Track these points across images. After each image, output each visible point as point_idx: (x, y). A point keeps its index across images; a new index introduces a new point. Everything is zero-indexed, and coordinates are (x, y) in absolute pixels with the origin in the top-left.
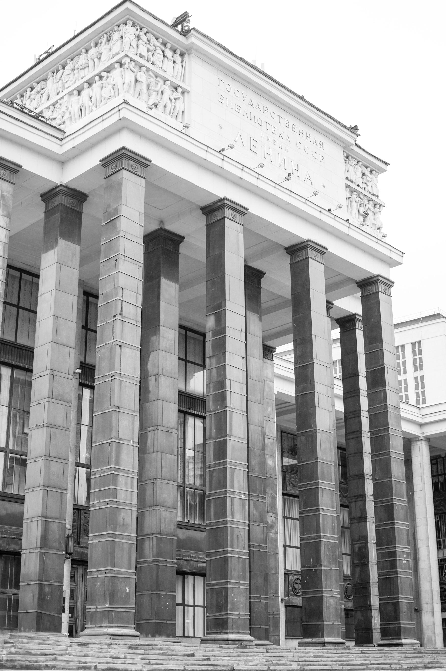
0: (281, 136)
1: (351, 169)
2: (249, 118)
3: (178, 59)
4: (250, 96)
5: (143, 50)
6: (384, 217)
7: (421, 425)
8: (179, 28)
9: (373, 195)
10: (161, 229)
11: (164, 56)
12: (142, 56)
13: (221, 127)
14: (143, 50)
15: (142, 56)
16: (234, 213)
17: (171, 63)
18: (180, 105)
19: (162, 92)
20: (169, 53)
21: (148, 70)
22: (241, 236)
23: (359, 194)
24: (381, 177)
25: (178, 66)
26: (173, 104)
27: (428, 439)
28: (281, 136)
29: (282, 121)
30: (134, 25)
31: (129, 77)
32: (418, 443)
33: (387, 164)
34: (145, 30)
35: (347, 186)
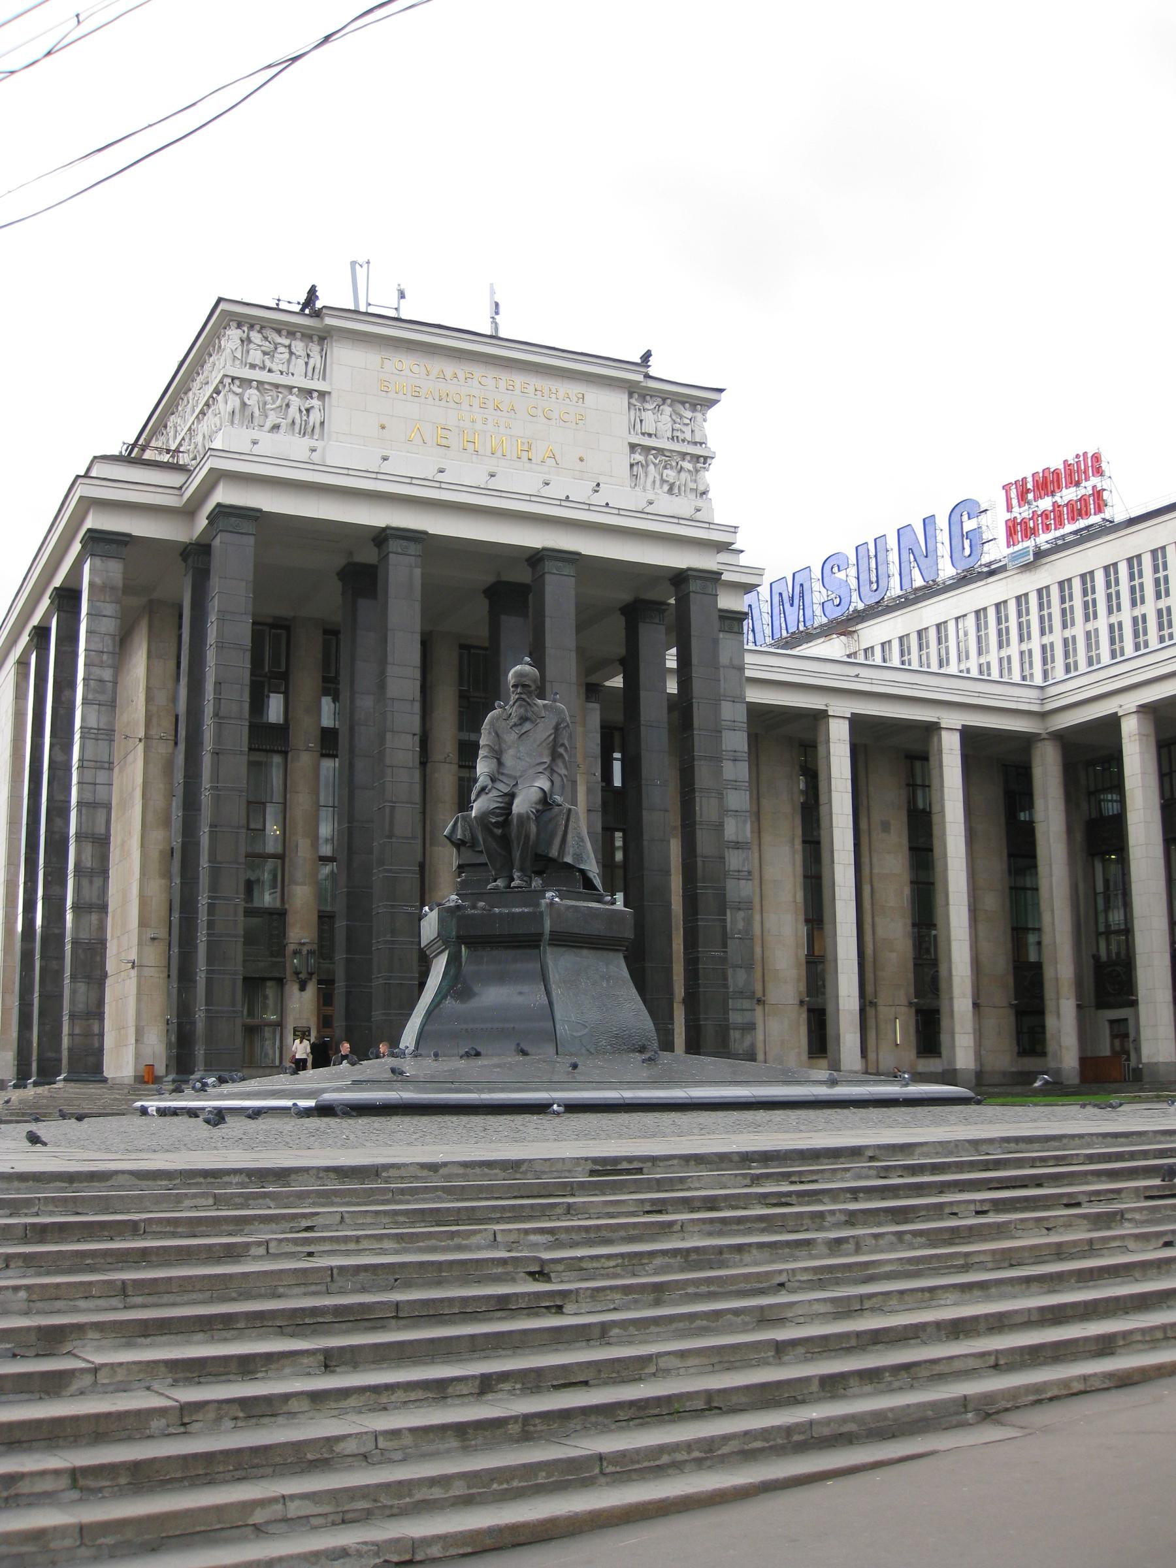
0: (497, 408)
1: (648, 416)
2: (437, 398)
3: (315, 349)
4: (438, 365)
5: (256, 356)
6: (712, 477)
7: (1043, 715)
8: (307, 311)
9: (695, 443)
10: (349, 564)
11: (291, 353)
12: (253, 366)
13: (383, 428)
14: (256, 356)
15: (253, 366)
16: (405, 543)
17: (301, 362)
18: (315, 417)
19: (288, 405)
20: (298, 346)
21: (260, 383)
22: (418, 572)
23: (661, 451)
24: (712, 413)
25: (316, 360)
26: (305, 418)
27: (1064, 738)
28: (497, 408)
29: (502, 385)
30: (239, 326)
31: (234, 402)
32: (1039, 744)
33: (721, 391)
34: (258, 327)
35: (633, 447)
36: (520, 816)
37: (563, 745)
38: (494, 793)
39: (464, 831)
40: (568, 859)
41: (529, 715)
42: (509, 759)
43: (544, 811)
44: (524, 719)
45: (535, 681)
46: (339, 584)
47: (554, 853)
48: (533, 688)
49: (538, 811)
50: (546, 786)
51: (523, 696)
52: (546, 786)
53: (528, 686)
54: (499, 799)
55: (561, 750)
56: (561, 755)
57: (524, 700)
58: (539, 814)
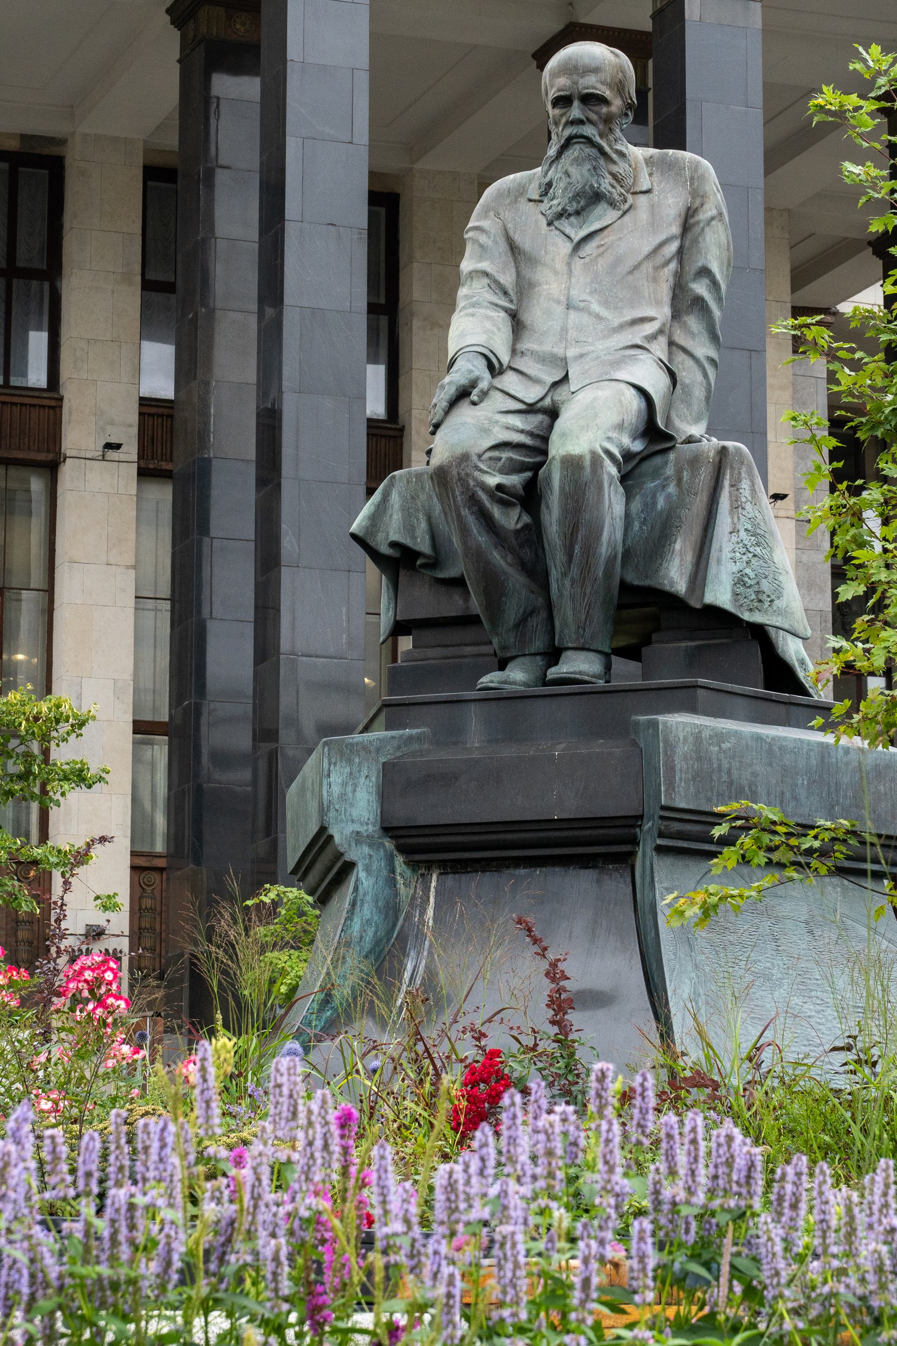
36: (572, 464)
37: (705, 272)
38: (498, 401)
39: (408, 513)
40: (719, 594)
41: (606, 184)
42: (543, 314)
43: (644, 457)
44: (591, 198)
45: (620, 87)
46: (168, 18)
47: (675, 575)
48: (617, 104)
49: (628, 456)
50: (656, 383)
51: (589, 131)
52: (656, 383)
53: (602, 100)
54: (517, 421)
55: (700, 288)
56: (699, 303)
57: (589, 141)
58: (632, 469)
